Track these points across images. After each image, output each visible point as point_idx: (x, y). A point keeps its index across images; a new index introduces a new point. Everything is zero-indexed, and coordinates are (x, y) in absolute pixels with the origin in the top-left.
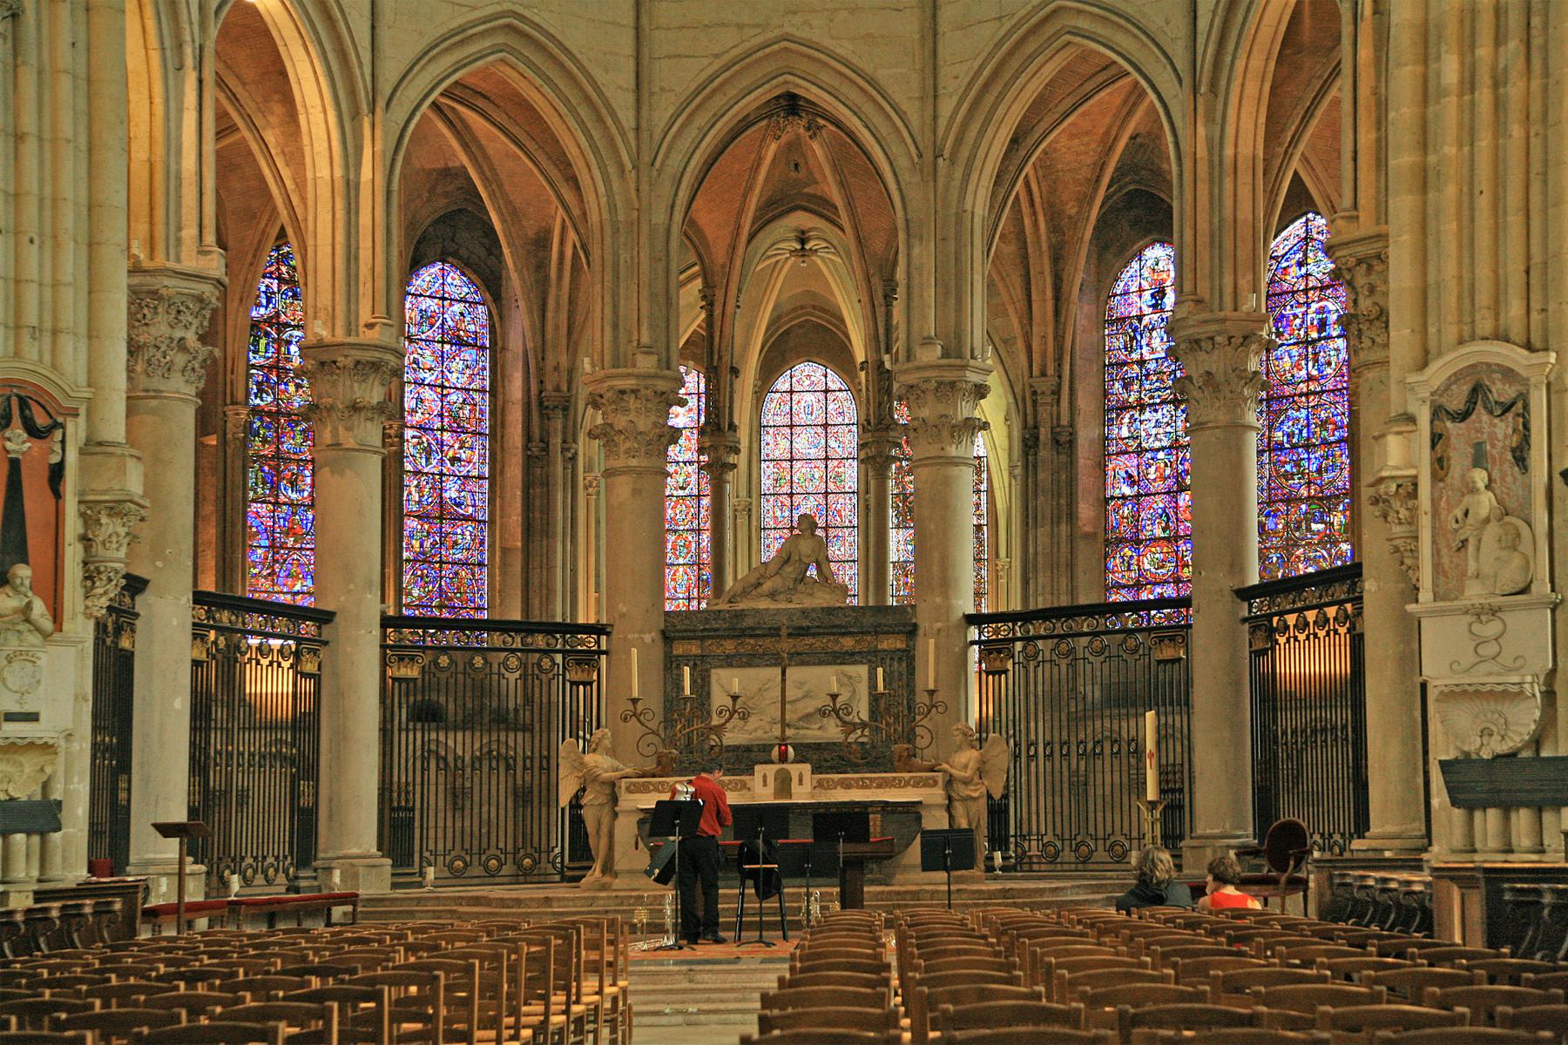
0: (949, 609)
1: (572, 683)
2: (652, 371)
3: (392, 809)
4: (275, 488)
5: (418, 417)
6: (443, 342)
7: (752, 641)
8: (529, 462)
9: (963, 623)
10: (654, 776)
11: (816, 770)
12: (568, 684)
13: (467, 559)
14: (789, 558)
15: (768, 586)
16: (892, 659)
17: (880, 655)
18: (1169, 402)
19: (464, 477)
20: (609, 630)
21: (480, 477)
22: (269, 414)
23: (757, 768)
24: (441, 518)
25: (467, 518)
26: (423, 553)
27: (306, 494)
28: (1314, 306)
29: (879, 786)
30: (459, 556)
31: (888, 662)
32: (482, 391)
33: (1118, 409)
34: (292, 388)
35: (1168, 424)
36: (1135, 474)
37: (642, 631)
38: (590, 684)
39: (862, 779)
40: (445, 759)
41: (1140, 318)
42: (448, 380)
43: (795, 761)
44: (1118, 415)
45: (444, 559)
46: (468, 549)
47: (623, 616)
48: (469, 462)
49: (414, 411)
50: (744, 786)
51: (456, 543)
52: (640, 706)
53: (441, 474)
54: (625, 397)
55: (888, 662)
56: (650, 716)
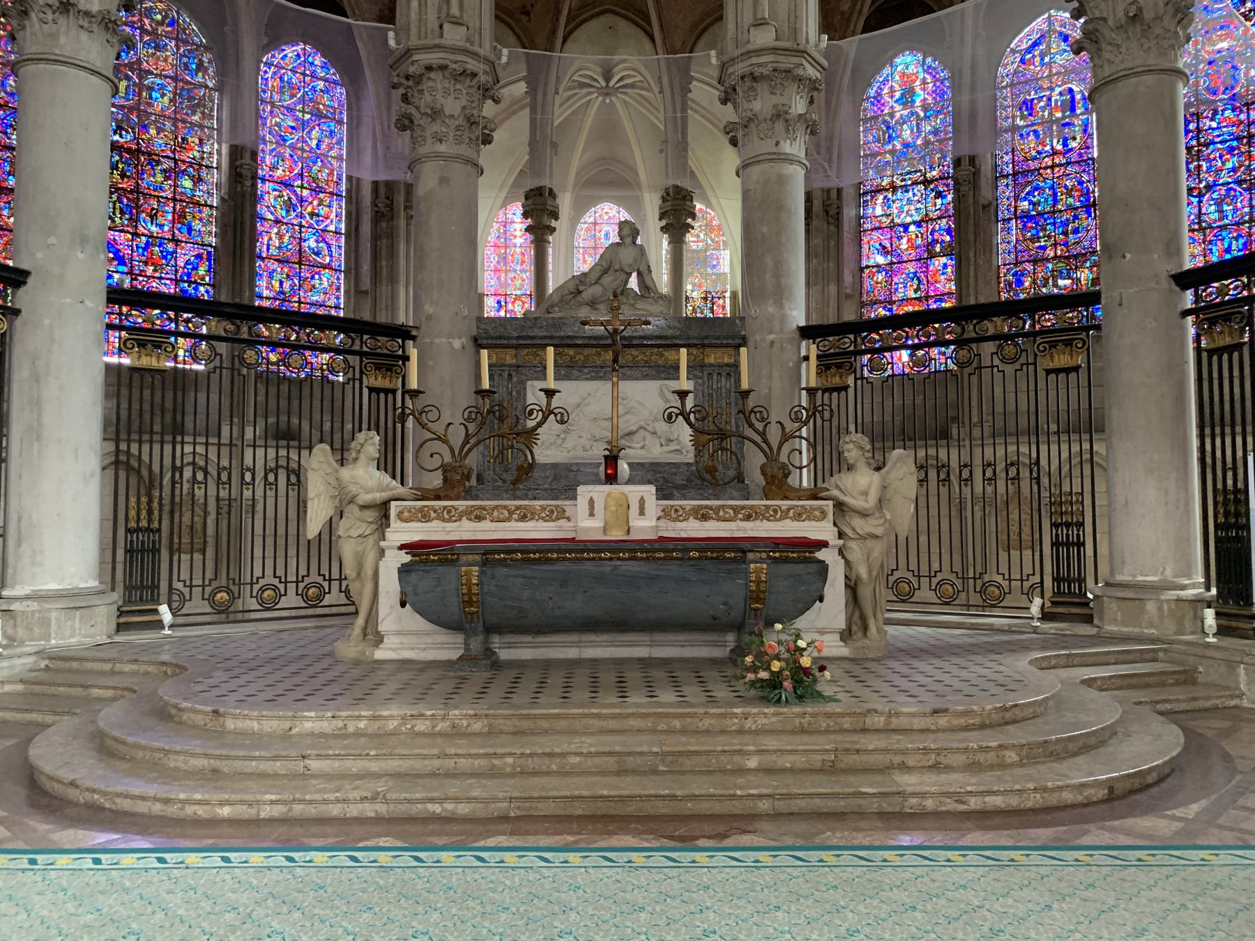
0: (783, 319)
1: (371, 390)
2: (461, 44)
3: (128, 530)
4: (134, 221)
5: (279, 173)
6: (303, 112)
7: (571, 352)
8: (378, 217)
9: (797, 335)
10: (438, 498)
11: (662, 494)
12: (365, 391)
13: (324, 301)
14: (609, 269)
15: (588, 294)
16: (719, 374)
17: (708, 370)
18: (920, 183)
19: (322, 230)
20: (414, 333)
21: (337, 232)
22: (129, 151)
23: (580, 489)
24: (300, 263)
25: (325, 267)
26: (282, 293)
27: (166, 228)
28: (1058, 90)
29: (748, 518)
30: (314, 298)
31: (715, 377)
32: (339, 158)
33: (871, 192)
34: (153, 132)
35: (919, 202)
36: (888, 245)
37: (450, 336)
38: (394, 392)
39: (723, 507)
40: (139, 472)
41: (892, 115)
42: (308, 145)
43: (626, 483)
44: (872, 197)
45: (302, 300)
46: (325, 293)
47: (429, 317)
48: (327, 218)
49: (274, 168)
50: (561, 515)
51: (314, 286)
52: (421, 402)
53: (301, 226)
54: (433, 75)
55: (715, 377)
56: (433, 415)
